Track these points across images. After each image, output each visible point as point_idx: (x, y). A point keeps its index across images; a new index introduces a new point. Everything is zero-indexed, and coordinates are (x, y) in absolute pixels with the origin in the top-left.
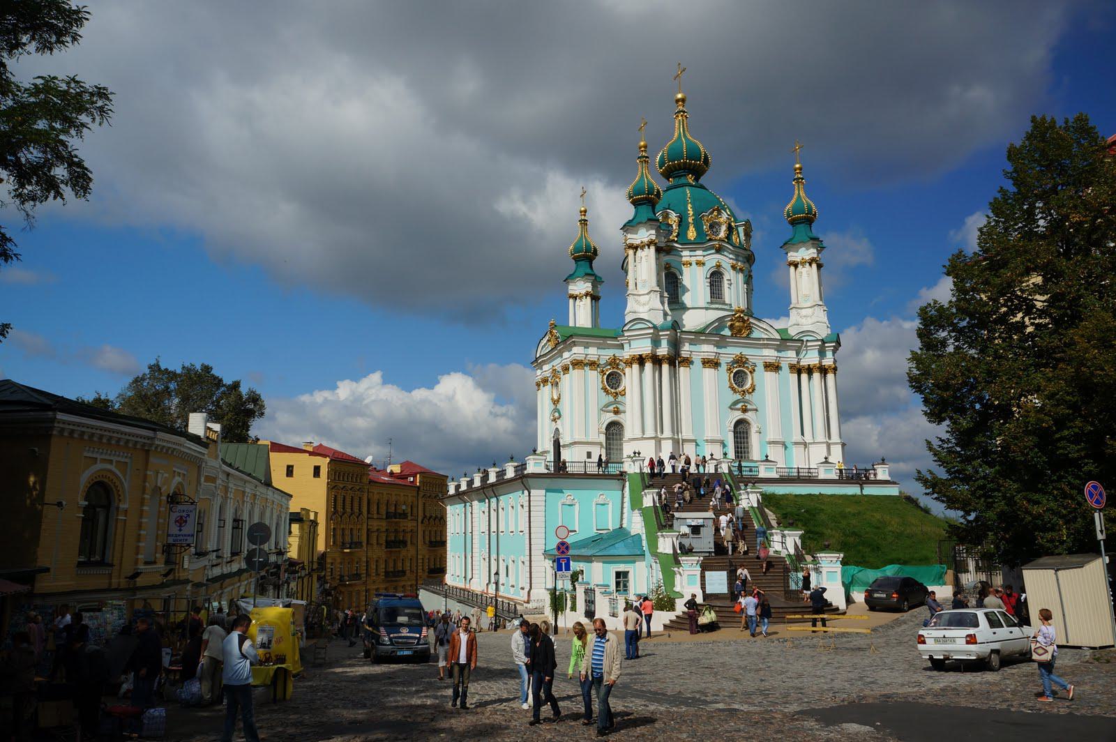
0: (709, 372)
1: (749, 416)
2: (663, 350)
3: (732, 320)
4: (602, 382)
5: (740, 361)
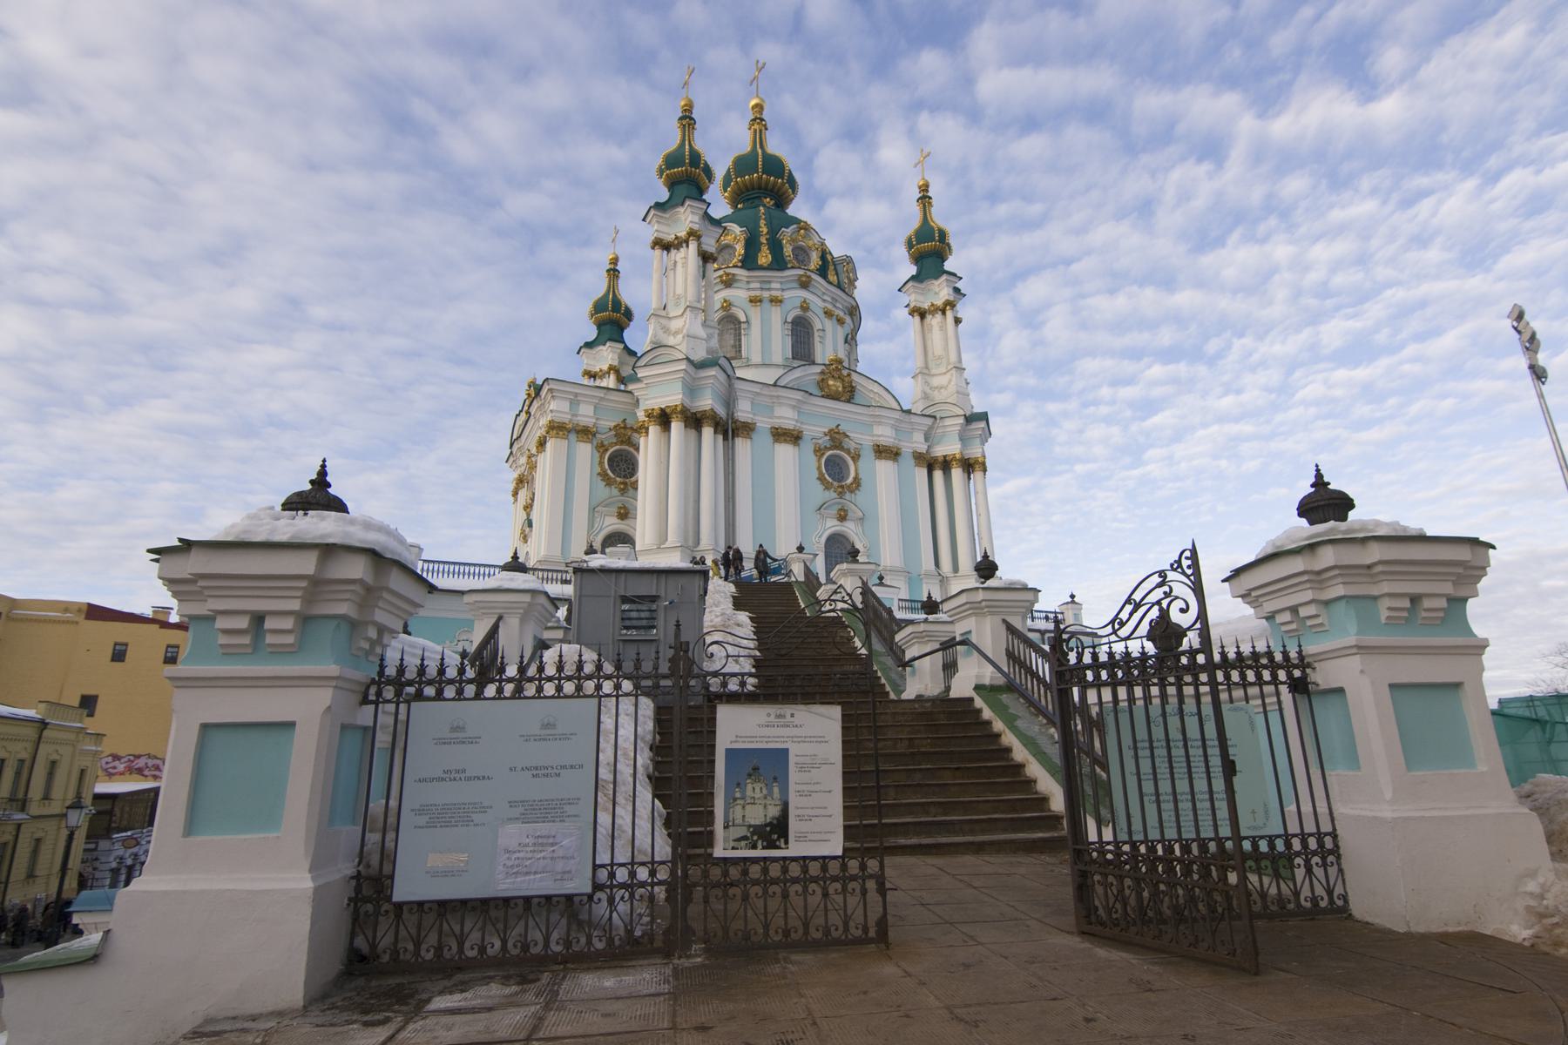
0: (785, 451)
1: (850, 529)
2: (707, 402)
3: (822, 373)
4: (601, 463)
5: (837, 438)
